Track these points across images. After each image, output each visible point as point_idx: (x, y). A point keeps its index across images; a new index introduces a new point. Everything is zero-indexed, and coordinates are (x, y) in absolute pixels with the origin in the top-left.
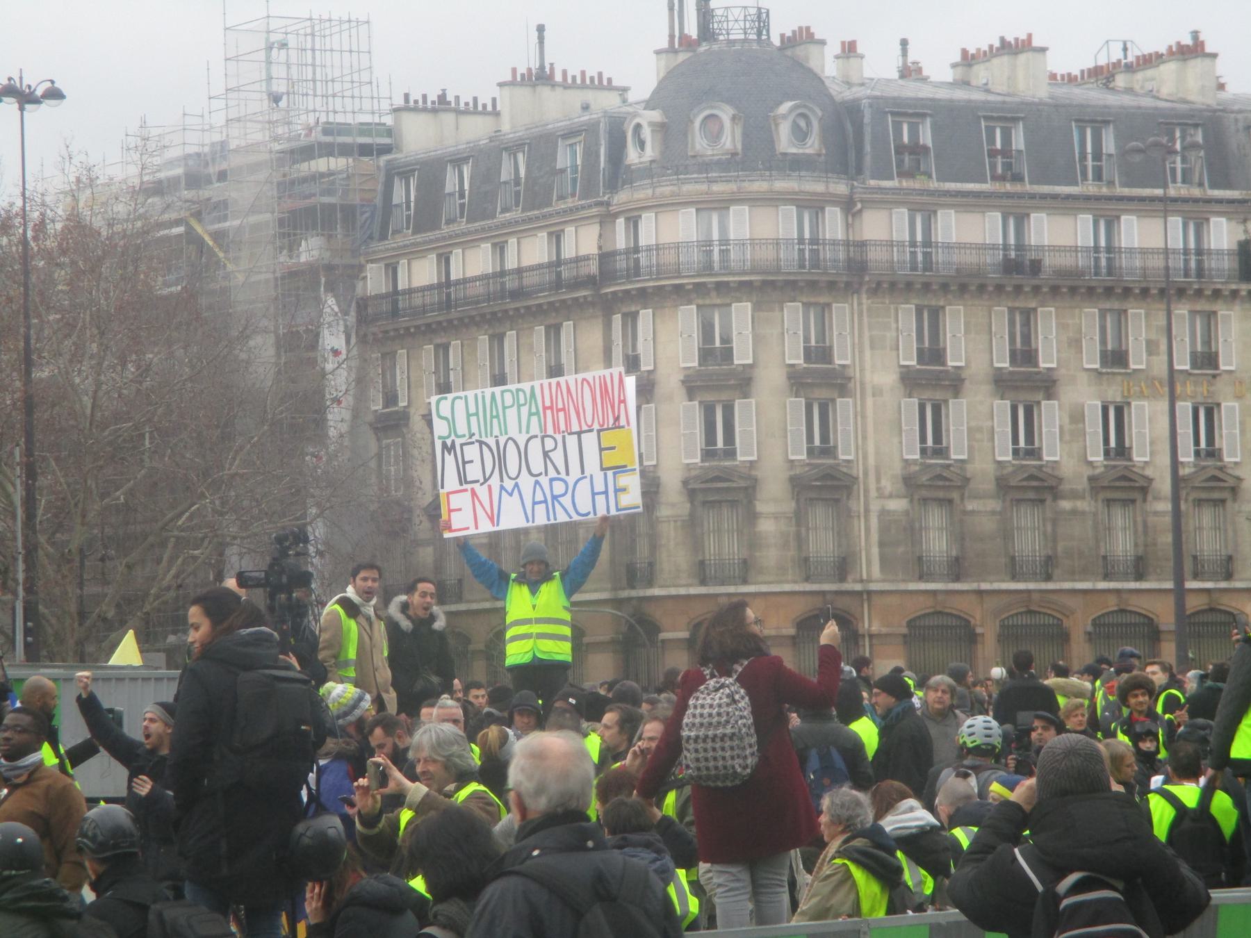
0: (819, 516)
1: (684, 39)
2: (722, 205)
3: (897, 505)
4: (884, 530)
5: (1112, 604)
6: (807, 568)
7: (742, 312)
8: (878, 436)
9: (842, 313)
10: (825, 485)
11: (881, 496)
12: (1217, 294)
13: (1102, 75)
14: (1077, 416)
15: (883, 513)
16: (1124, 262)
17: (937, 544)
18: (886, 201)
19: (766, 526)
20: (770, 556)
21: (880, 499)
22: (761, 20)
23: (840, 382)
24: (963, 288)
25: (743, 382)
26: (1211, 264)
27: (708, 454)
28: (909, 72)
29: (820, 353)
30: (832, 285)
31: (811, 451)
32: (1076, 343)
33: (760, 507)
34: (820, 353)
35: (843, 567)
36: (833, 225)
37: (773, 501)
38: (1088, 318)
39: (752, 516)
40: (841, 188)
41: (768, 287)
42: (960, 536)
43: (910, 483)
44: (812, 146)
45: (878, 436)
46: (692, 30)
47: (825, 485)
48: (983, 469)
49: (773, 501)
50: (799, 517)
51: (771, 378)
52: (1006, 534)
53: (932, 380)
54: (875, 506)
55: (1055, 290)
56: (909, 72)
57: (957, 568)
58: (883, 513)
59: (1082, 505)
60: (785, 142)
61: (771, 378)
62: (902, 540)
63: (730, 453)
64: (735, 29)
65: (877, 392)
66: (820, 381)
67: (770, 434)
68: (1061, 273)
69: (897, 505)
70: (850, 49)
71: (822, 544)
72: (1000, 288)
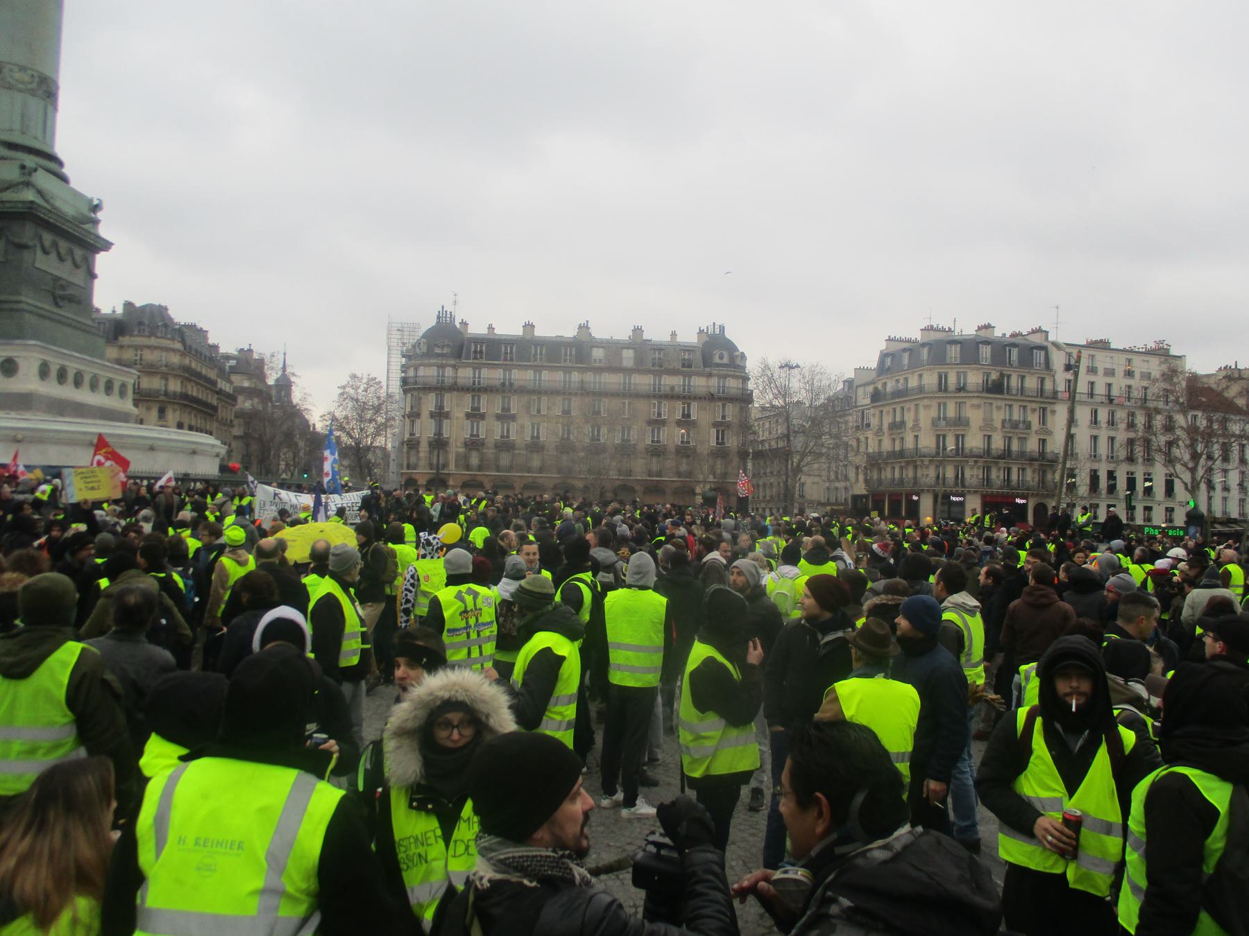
3: (462, 450)
5: (530, 480)
8: (457, 431)
9: (447, 396)
10: (439, 444)
14: (523, 427)
17: (474, 460)
18: (468, 365)
19: (422, 455)
20: (422, 463)
21: (456, 448)
23: (447, 416)
25: (418, 415)
29: (440, 407)
34: (440, 407)
35: (445, 466)
36: (449, 372)
37: (424, 447)
38: (525, 398)
39: (418, 452)
40: (453, 362)
42: (481, 460)
43: (466, 444)
45: (457, 431)
47: (439, 444)
48: (490, 441)
49: (424, 447)
50: (431, 452)
52: (497, 459)
53: (475, 415)
57: (480, 468)
59: (523, 452)
62: (464, 462)
66: (440, 415)
67: (426, 429)
69: (462, 450)
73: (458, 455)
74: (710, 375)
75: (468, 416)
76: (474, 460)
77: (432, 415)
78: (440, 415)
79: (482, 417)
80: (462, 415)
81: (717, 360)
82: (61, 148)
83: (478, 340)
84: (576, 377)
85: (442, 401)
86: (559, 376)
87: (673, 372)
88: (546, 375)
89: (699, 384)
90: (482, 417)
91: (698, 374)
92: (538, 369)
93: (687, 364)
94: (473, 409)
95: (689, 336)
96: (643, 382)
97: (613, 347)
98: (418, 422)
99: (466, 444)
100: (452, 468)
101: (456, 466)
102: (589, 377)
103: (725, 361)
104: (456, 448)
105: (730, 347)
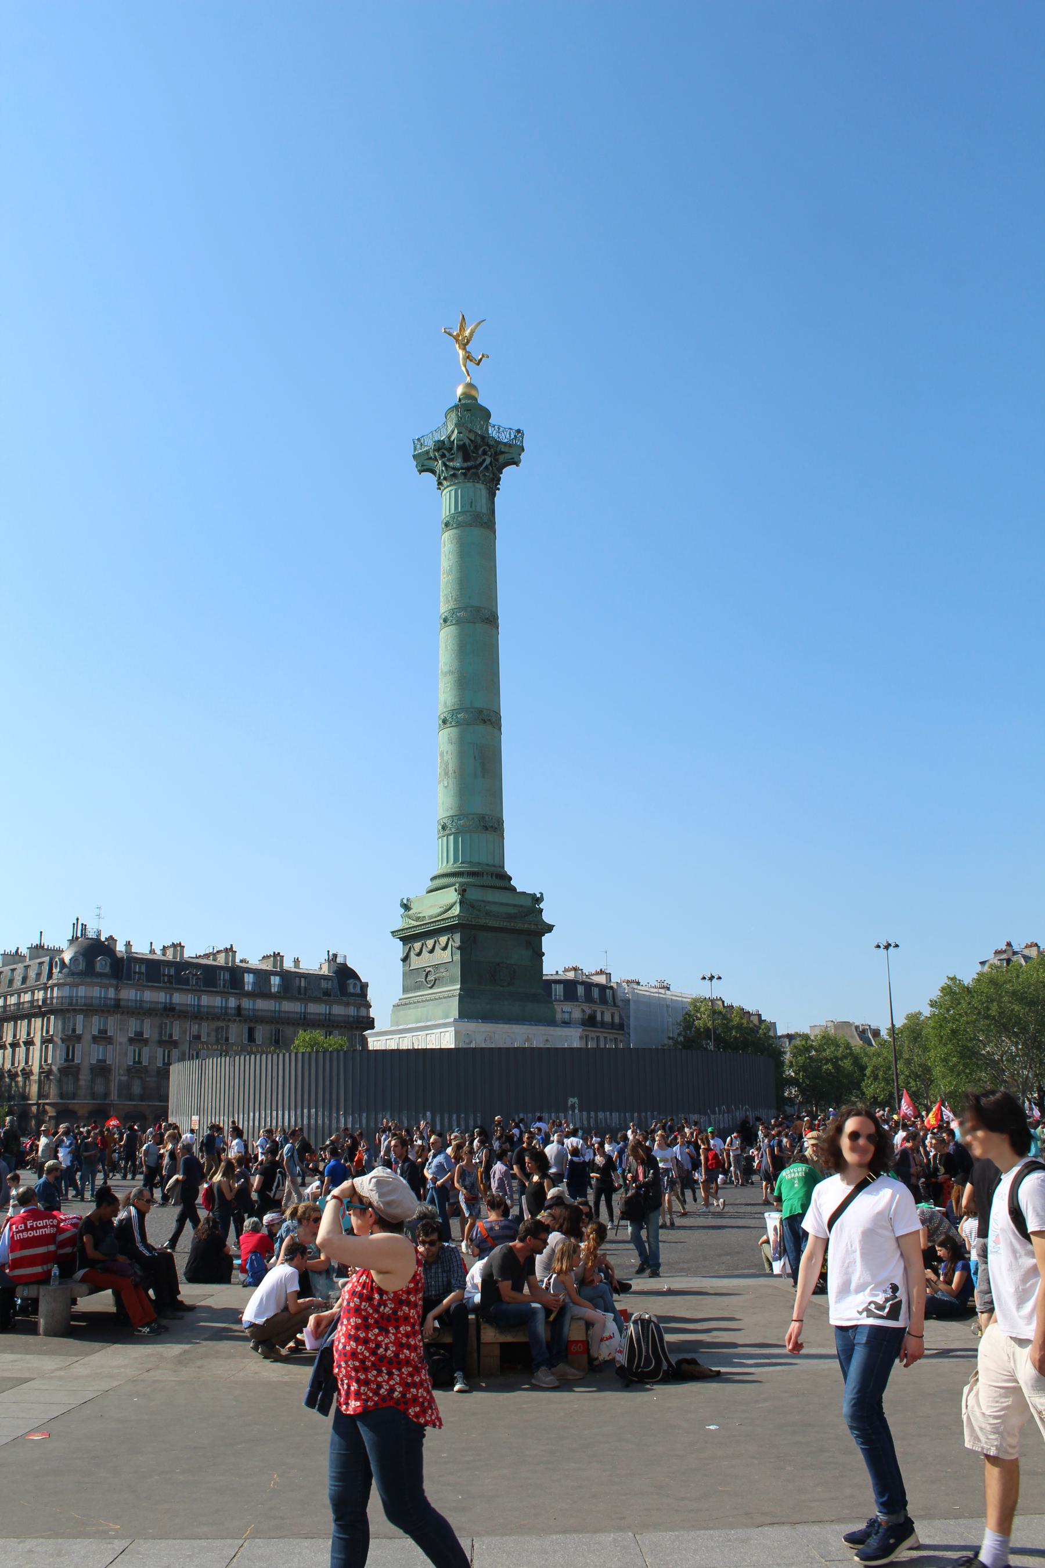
0: (99, 1081)
1: (77, 938)
2: (77, 986)
4: (119, 1086)
6: (93, 1096)
7: (80, 1018)
11: (119, 1075)
12: (229, 1020)
13: (207, 956)
15: (120, 1080)
16: (202, 1010)
17: (137, 1089)
19: (82, 1083)
21: (118, 1077)
22: (99, 933)
24: (150, 1014)
25: (79, 1038)
26: (230, 1011)
27: (66, 1060)
28: (152, 951)
30: (109, 1011)
31: (134, 1062)
32: (185, 1032)
33: (80, 1077)
35: (106, 1095)
36: (111, 993)
37: (84, 1077)
39: (77, 1080)
41: (89, 1009)
44: (107, 970)
46: (79, 935)
49: (84, 1077)
50: (93, 1080)
51: (87, 1038)
54: (117, 1078)
55: (179, 1016)
56: (152, 951)
57: (142, 1098)
58: (120, 1080)
60: (98, 968)
61: (87, 1038)
62: (125, 1091)
63: (73, 1060)
64: (91, 934)
65: (120, 1044)
68: (180, 1011)
70: (128, 944)
71: (99, 1088)
72: (162, 1015)
73: (120, 1083)
74: (347, 1004)
75: (131, 1040)
76: (137, 1089)
77: (95, 1039)
78: (71, 1039)
79: (146, 1042)
80: (124, 1040)
81: (351, 990)
82: (509, 869)
83: (132, 960)
84: (232, 1002)
85: (106, 1024)
86: (218, 1001)
87: (317, 1000)
88: (205, 1000)
89: (338, 1010)
90: (146, 1042)
91: (339, 1003)
92: (197, 991)
93: (327, 993)
94: (100, 1031)
95: (314, 963)
96: (289, 1007)
97: (262, 976)
98: (78, 1047)
99: (129, 1070)
100: (114, 1095)
101: (119, 1096)
102: (246, 1004)
103: (358, 991)
104: (118, 1077)
105: (353, 975)
